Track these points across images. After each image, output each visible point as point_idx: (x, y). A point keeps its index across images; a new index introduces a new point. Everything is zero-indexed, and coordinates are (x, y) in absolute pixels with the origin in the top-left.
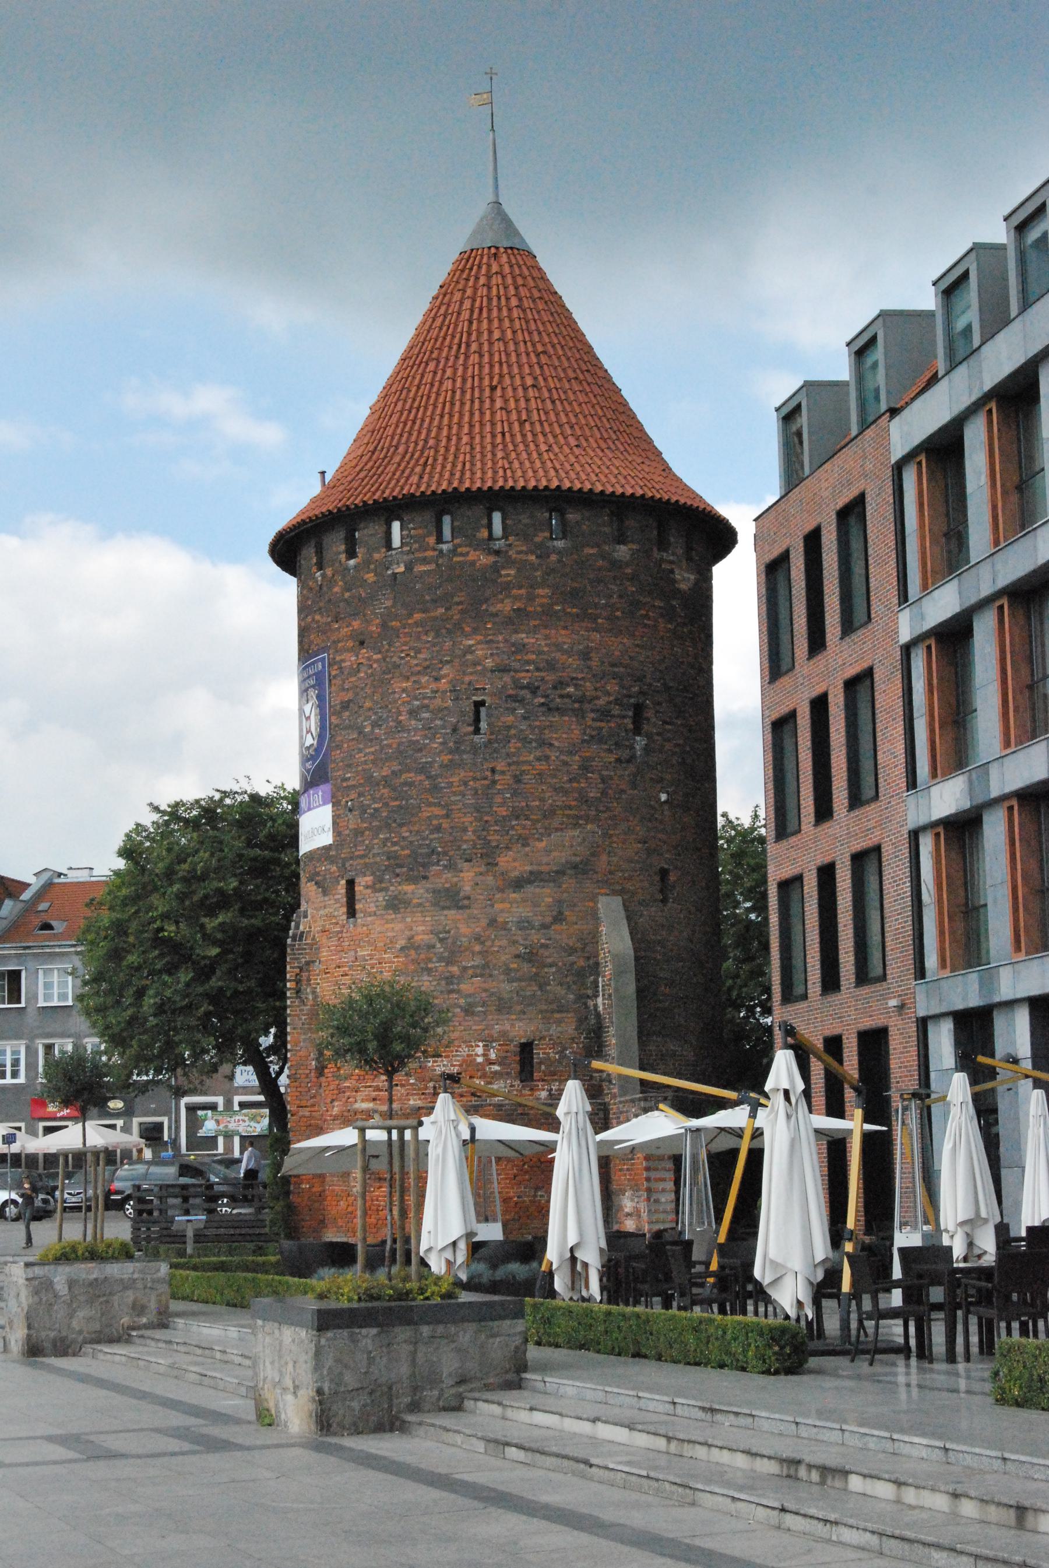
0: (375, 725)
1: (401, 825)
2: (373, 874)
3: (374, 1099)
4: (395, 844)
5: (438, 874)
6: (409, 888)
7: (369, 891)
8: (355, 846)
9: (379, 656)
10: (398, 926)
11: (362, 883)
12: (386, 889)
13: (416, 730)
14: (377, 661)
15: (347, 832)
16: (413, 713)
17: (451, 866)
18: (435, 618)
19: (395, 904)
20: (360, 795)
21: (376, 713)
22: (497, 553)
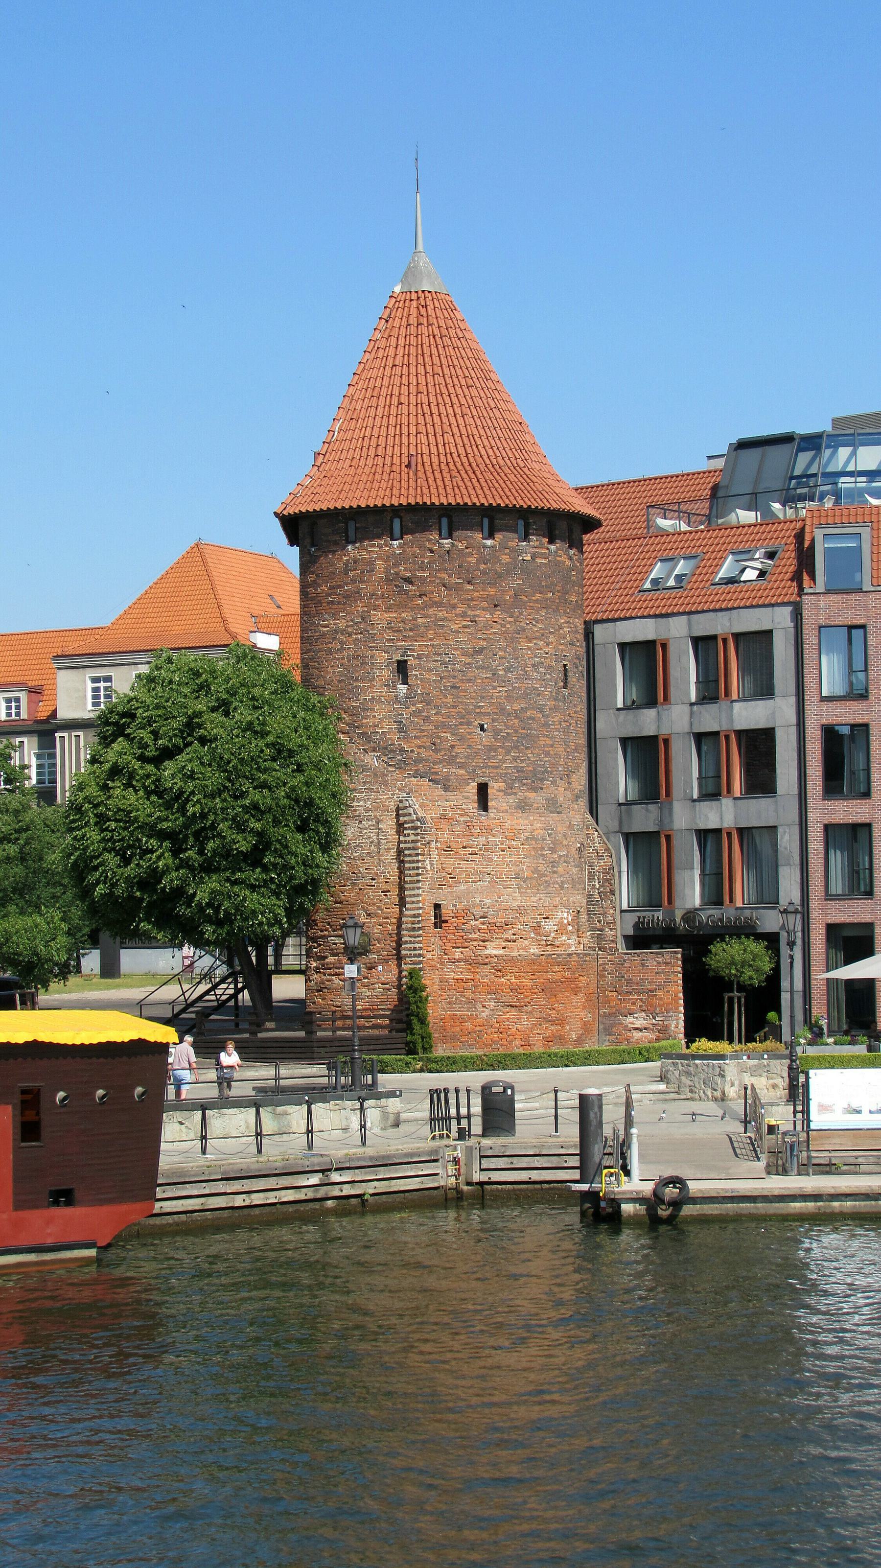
0: (507, 670)
1: (527, 748)
2: (505, 781)
3: (504, 948)
4: (522, 761)
6: (531, 795)
7: (502, 794)
8: (489, 758)
9: (512, 619)
10: (523, 822)
12: (515, 794)
13: (536, 679)
14: (509, 622)
15: (480, 747)
17: (554, 782)
18: (547, 599)
19: (523, 806)
20: (493, 720)
21: (508, 662)
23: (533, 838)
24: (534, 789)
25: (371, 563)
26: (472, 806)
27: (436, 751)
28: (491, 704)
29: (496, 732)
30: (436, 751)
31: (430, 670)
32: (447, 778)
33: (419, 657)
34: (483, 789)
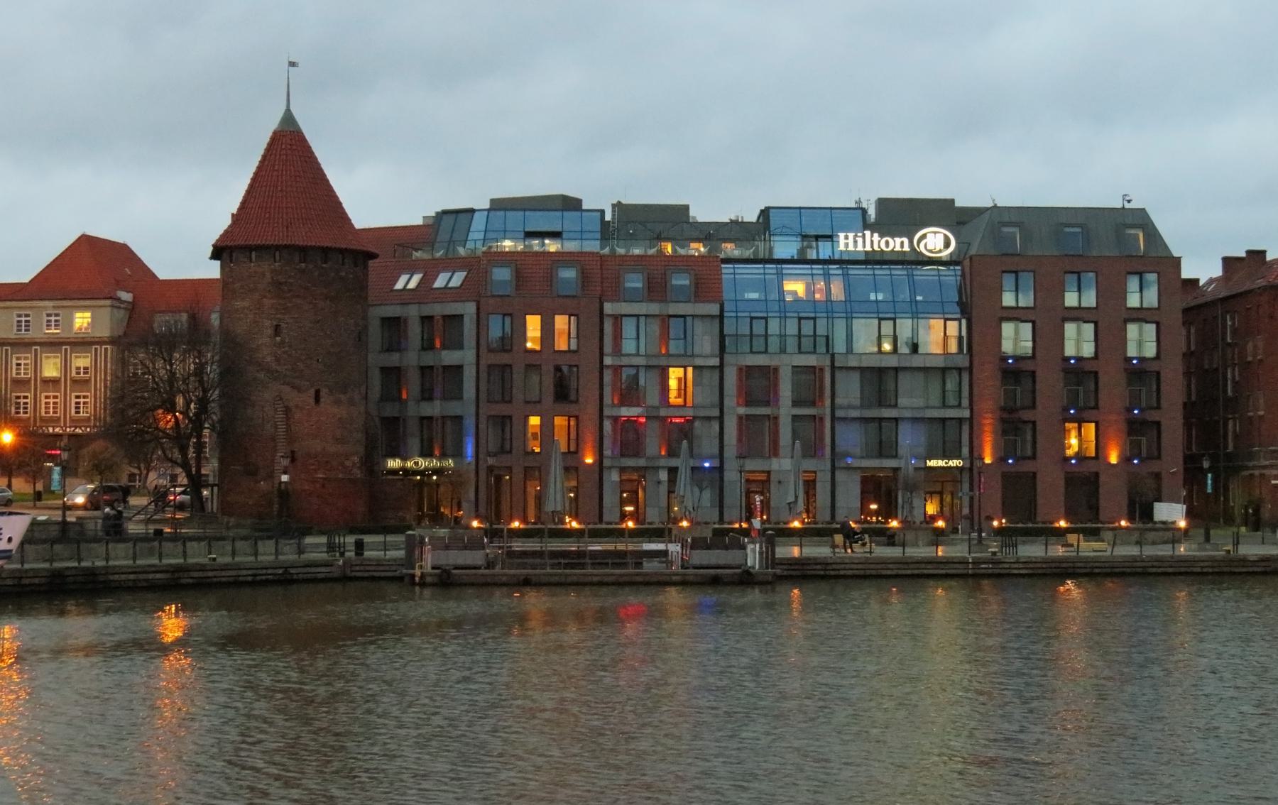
11: (324, 392)
19: (337, 402)
26: (312, 401)
34: (317, 393)
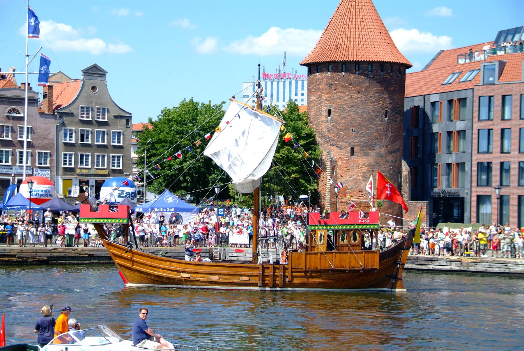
5: (377, 149)
16: (373, 111)
17: (380, 147)
19: (366, 155)
22: (391, 76)
23: (370, 165)
24: (371, 150)
25: (322, 79)
26: (349, 155)
27: (338, 137)
28: (356, 123)
29: (358, 132)
30: (338, 137)
31: (337, 112)
32: (341, 146)
33: (334, 108)
34: (352, 149)
